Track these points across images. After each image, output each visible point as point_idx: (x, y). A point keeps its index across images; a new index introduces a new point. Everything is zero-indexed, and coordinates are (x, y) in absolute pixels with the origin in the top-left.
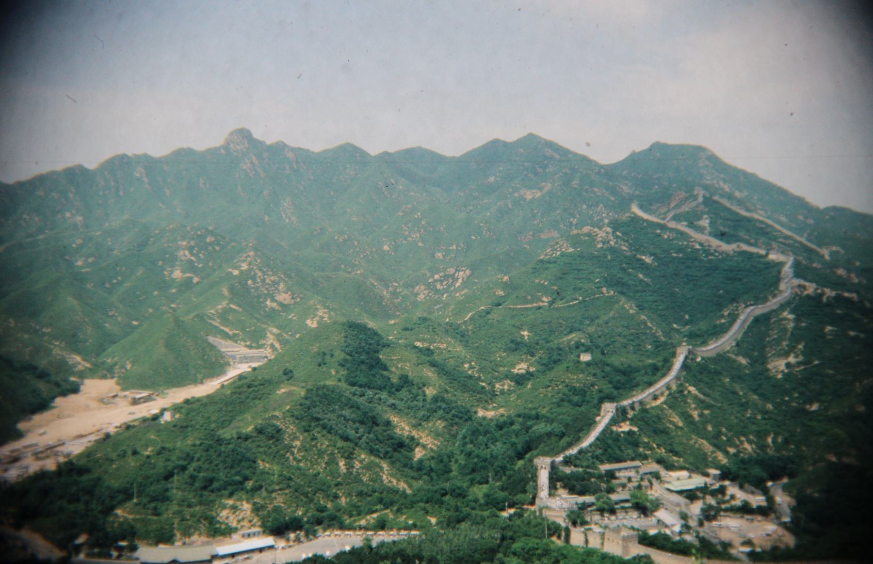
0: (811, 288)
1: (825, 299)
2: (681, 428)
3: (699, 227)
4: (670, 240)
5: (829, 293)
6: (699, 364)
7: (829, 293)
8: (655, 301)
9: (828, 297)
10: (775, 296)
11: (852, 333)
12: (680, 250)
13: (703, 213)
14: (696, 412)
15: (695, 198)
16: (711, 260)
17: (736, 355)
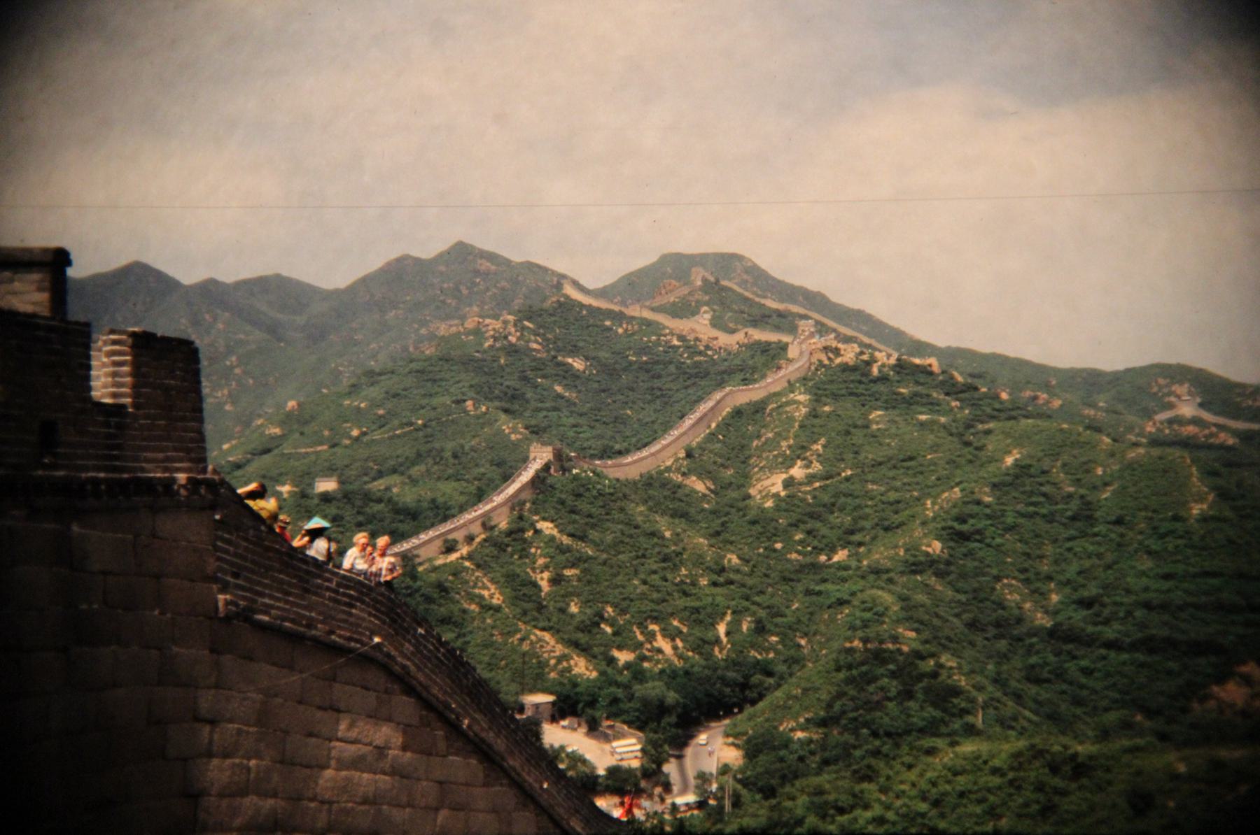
1: (875, 371)
2: (497, 609)
9: (883, 365)
12: (644, 350)
13: (699, 304)
14: (546, 575)
16: (700, 362)
17: (684, 474)
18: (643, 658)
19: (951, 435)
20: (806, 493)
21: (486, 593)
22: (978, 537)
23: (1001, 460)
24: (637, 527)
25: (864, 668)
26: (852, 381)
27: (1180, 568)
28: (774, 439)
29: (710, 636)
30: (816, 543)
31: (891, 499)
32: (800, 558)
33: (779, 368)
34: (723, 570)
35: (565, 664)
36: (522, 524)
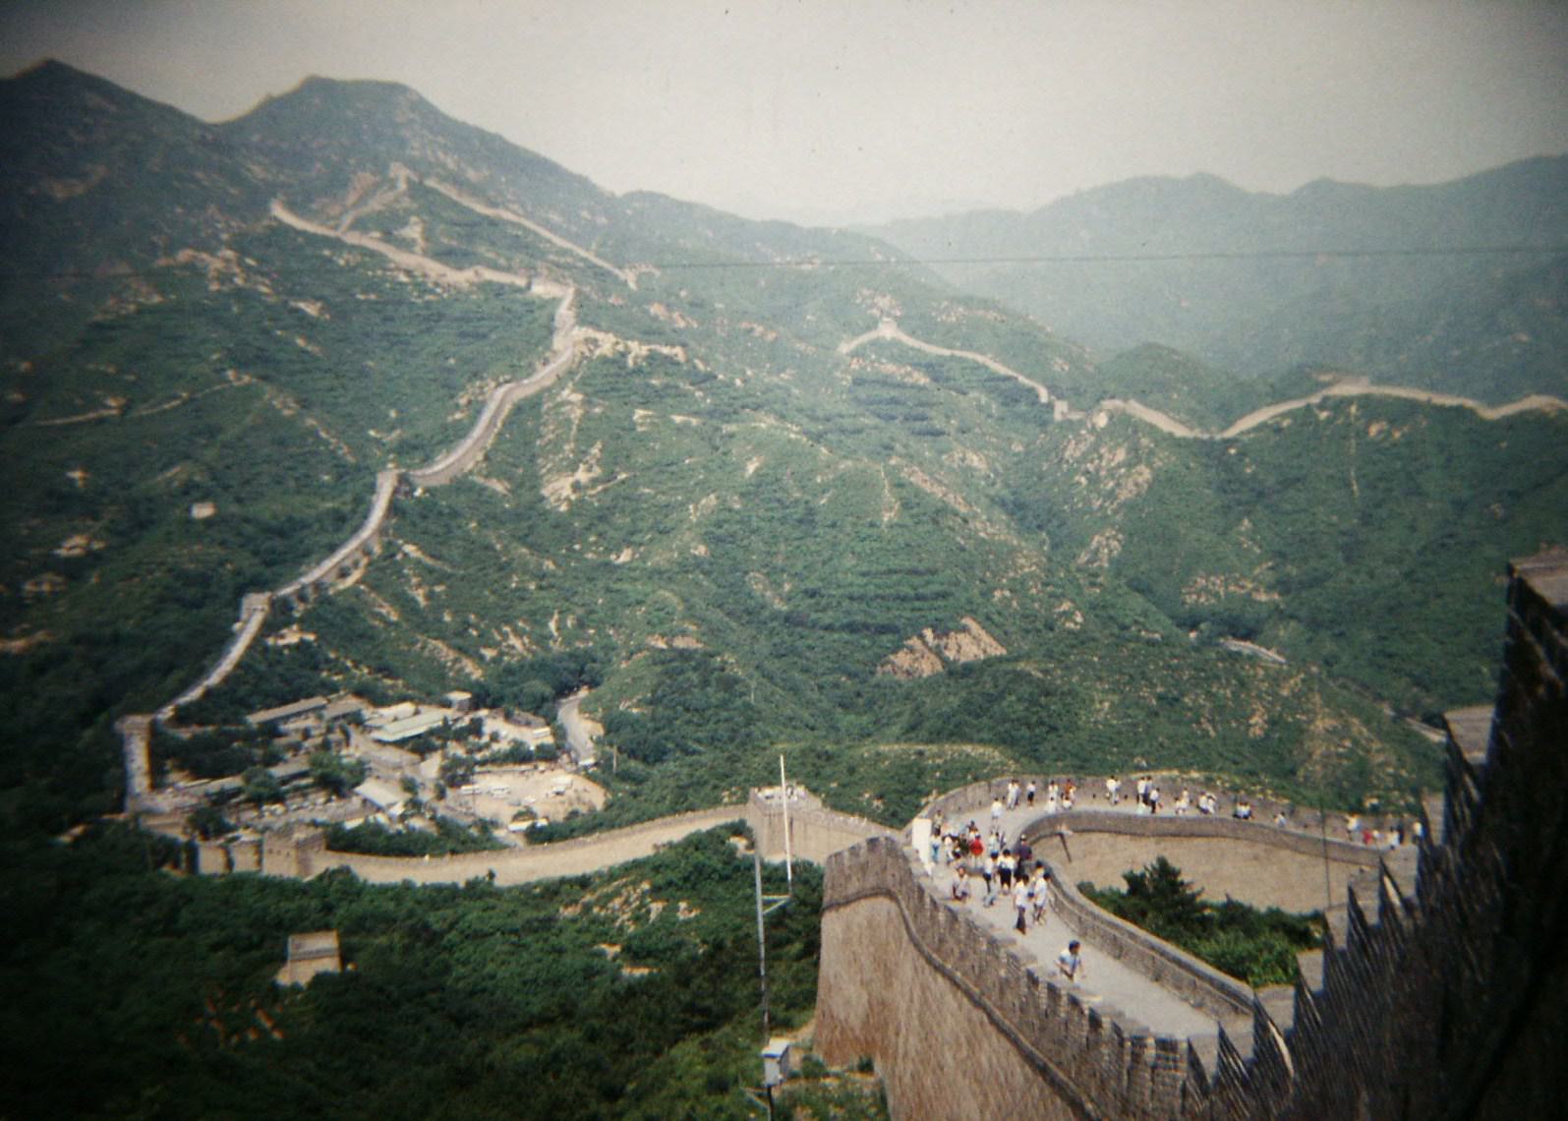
0: (607, 344)
1: (630, 362)
2: (396, 624)
3: (404, 240)
4: (351, 269)
5: (638, 350)
6: (419, 500)
7: (638, 350)
8: (332, 389)
9: (636, 357)
10: (546, 362)
11: (678, 419)
14: (421, 591)
15: (392, 184)
21: (384, 611)
23: (744, 469)
27: (874, 568)
29: (545, 632)
34: (543, 576)
36: (392, 550)
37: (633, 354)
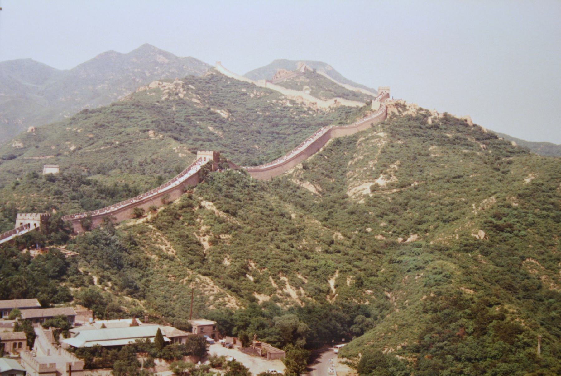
1: (430, 121)
2: (172, 259)
9: (435, 118)
14: (207, 238)
17: (301, 180)
18: (277, 300)
19: (486, 163)
20: (387, 195)
21: (163, 247)
22: (509, 229)
24: (271, 210)
25: (446, 311)
26: (415, 127)
28: (363, 160)
29: (323, 287)
30: (395, 229)
31: (447, 202)
32: (384, 238)
33: (365, 116)
34: (332, 242)
35: (221, 300)
37: (432, 117)
